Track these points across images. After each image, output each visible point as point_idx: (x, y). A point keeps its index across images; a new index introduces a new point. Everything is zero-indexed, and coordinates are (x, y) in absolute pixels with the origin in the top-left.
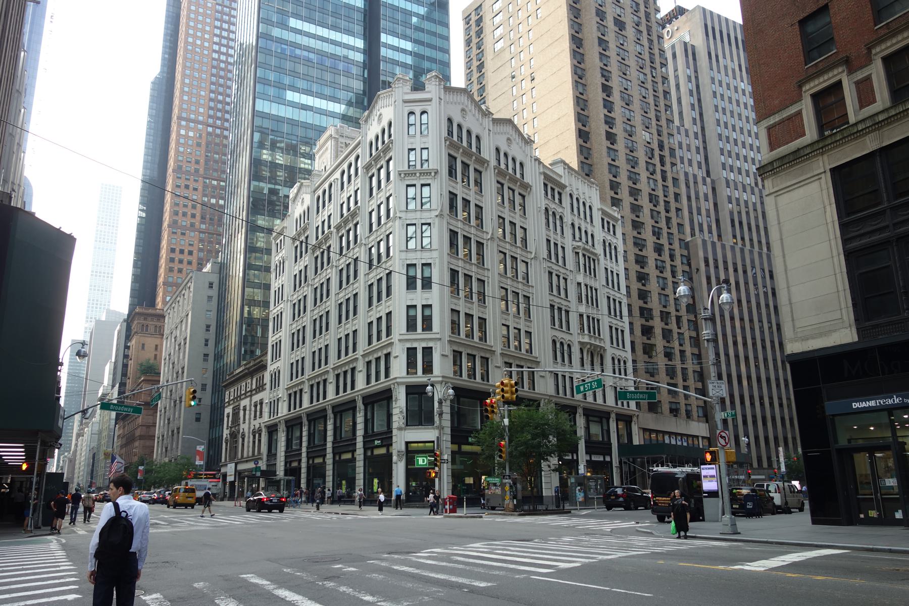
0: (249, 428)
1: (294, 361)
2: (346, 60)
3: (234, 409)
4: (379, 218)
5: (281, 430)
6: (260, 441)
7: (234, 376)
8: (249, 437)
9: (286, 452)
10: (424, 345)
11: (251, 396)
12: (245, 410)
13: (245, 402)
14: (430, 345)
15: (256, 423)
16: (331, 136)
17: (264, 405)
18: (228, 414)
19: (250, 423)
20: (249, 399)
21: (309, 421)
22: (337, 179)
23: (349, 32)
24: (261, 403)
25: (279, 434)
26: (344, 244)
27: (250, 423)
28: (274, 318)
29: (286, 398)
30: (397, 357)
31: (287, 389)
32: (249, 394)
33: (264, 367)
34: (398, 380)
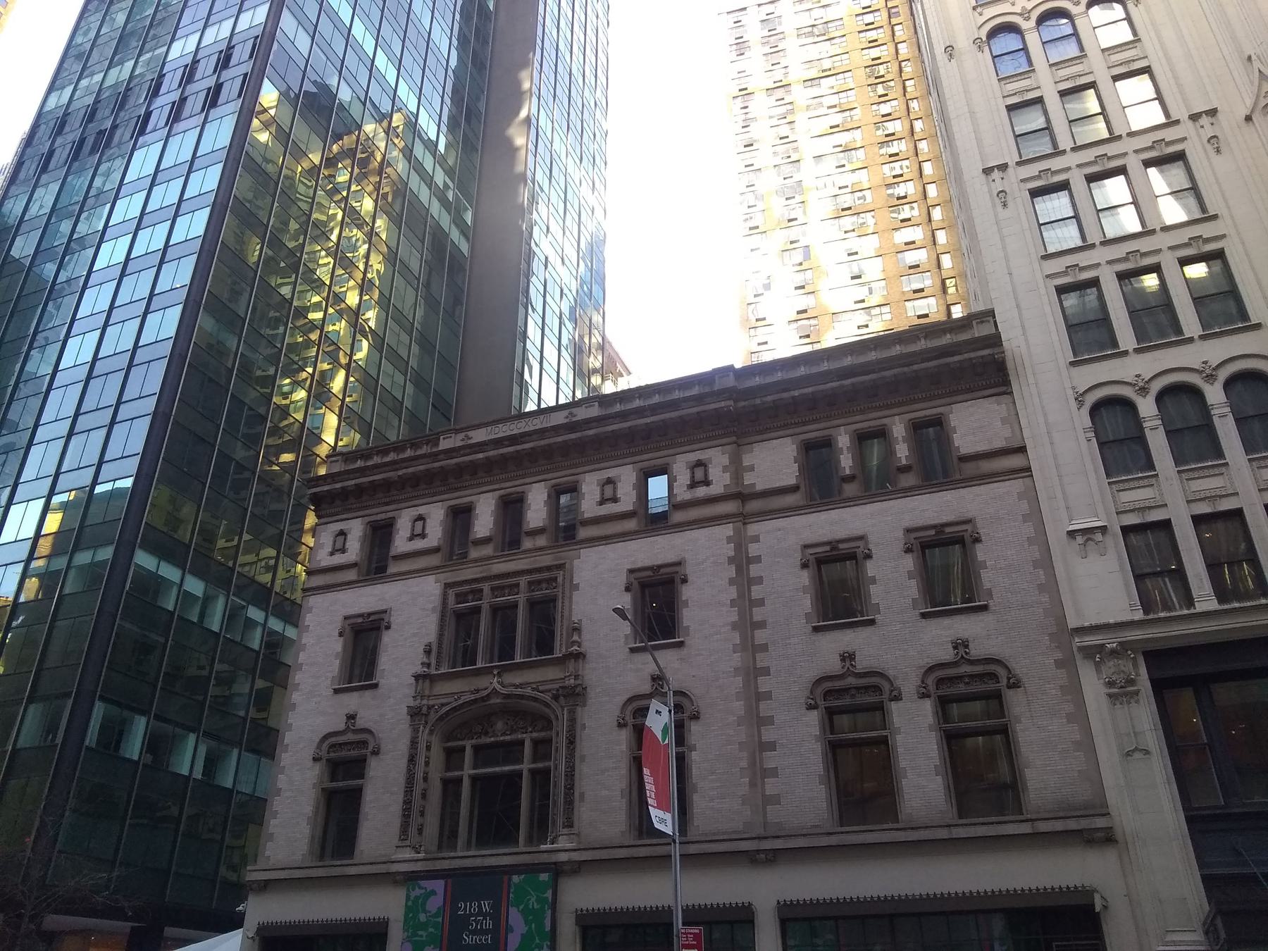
7: (435, 456)
11: (744, 518)
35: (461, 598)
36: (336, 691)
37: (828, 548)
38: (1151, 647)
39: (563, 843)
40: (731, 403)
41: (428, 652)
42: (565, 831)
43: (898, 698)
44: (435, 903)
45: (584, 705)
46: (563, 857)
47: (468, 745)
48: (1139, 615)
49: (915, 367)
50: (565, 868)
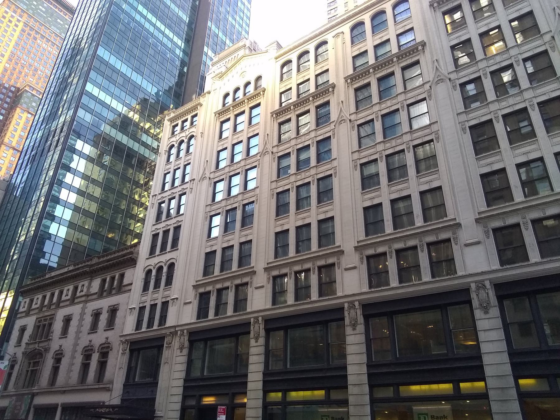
0: (76, 345)
3: (39, 320)
6: (102, 365)
8: (73, 357)
9: (186, 381)
11: (86, 302)
12: (67, 320)
13: (75, 310)
15: (98, 339)
16: (245, 46)
17: (119, 314)
18: (23, 330)
20: (81, 305)
22: (343, 33)
24: (113, 311)
25: (166, 353)
27: (77, 338)
31: (195, 287)
33: (132, 262)
35: (39, 322)
36: (60, 338)
37: (96, 311)
38: (132, 341)
39: (36, 388)
40: (88, 269)
41: (30, 337)
42: (37, 385)
43: (94, 353)
44: (13, 402)
45: (48, 353)
46: (35, 391)
47: (32, 361)
48: (134, 332)
49: (119, 259)
50: (35, 394)
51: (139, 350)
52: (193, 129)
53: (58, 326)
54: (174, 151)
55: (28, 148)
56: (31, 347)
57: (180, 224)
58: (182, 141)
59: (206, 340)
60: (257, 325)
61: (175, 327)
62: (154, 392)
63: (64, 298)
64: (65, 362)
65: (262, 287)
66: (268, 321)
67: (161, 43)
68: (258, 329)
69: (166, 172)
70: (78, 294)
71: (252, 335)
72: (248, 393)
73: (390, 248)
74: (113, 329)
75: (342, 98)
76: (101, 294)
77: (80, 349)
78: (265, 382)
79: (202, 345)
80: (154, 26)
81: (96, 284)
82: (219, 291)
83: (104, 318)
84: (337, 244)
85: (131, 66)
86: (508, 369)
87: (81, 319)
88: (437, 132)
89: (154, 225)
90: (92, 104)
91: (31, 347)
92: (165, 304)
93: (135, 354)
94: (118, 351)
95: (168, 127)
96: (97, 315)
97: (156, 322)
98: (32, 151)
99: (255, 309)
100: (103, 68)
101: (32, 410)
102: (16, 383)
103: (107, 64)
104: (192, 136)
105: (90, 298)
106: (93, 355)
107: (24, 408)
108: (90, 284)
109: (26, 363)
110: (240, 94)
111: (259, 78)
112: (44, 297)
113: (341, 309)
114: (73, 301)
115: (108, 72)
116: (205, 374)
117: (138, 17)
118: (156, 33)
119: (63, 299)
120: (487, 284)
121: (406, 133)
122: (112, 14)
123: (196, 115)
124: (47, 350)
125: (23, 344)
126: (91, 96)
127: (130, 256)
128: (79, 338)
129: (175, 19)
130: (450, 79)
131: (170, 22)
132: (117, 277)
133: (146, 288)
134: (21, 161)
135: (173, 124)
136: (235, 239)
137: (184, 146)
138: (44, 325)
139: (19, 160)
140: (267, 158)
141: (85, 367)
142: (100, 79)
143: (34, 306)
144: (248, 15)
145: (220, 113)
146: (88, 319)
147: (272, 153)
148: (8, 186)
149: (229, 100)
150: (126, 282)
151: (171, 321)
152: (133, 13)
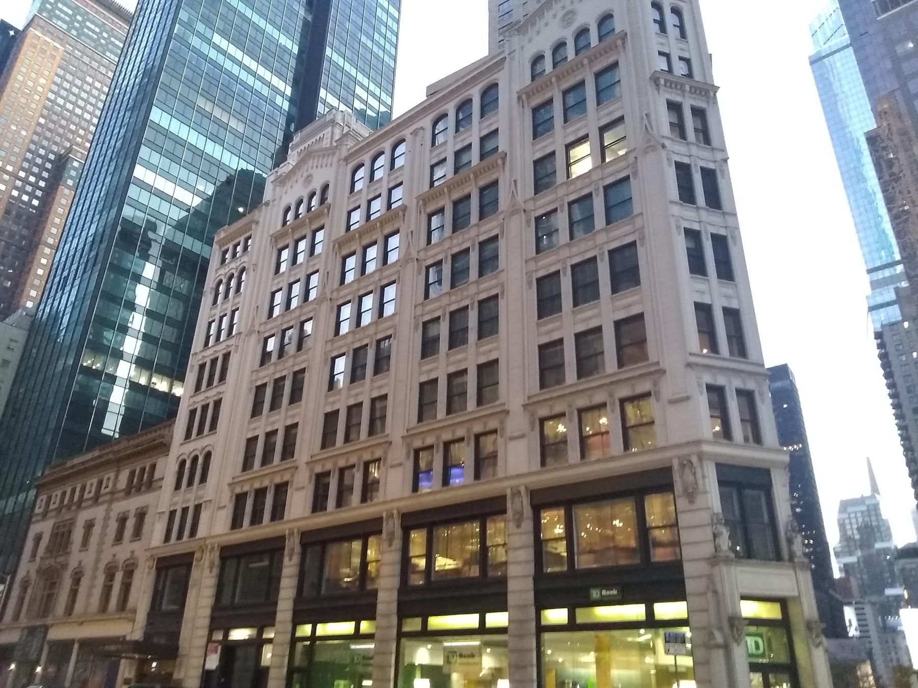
0: (98, 560)
1: (341, 404)
2: (272, 104)
3: (56, 527)
4: (219, 331)
5: (206, 563)
6: (126, 587)
10: (737, 383)
11: (111, 502)
13: (98, 513)
14: (750, 385)
15: (123, 552)
17: (147, 519)
18: (38, 538)
19: (99, 552)
20: (105, 507)
21: (304, 546)
22: (422, 128)
23: (280, 75)
24: (141, 516)
25: (195, 574)
26: (213, 331)
27: (99, 552)
28: (202, 367)
29: (227, 500)
30: (688, 398)
32: (107, 498)
33: (163, 447)
34: (706, 448)
48: (162, 545)
51: (167, 568)
52: (245, 259)
53: (78, 534)
54: (222, 288)
55: (58, 266)
56: (47, 562)
57: (221, 396)
58: (232, 276)
59: (239, 557)
60: (292, 539)
61: (204, 539)
62: (179, 623)
63: (86, 496)
64: (85, 582)
65: (303, 488)
66: (304, 535)
67: (252, 89)
68: (293, 545)
69: (210, 320)
70: (103, 491)
71: (286, 552)
72: (277, 624)
73: (611, 395)
74: (140, 540)
75: (413, 228)
76: (129, 491)
77: (102, 565)
78: (400, 604)
79: (235, 561)
80: (240, 64)
81: (124, 476)
82: (342, 471)
83: (130, 524)
84: (386, 433)
85: (205, 133)
86: (531, 596)
87: (105, 526)
88: (502, 286)
89: (192, 397)
90: (144, 197)
91: (47, 562)
92: (198, 508)
93: (163, 574)
94: (144, 569)
95: (217, 253)
96: (123, 520)
97: (187, 532)
98: (63, 270)
99: (292, 517)
100: (160, 139)
101: (46, 649)
102: (28, 611)
103: (166, 133)
104: (243, 270)
105: (116, 496)
106: (117, 574)
107: (35, 644)
108: (117, 477)
109: (42, 583)
110: (302, 209)
111: (325, 188)
112: (64, 494)
113: (503, 498)
114: (96, 500)
115: (168, 145)
116: (236, 600)
117: (213, 54)
118: (244, 75)
119: (85, 498)
120: (522, 489)
121: (473, 283)
122: (173, 54)
123: (250, 237)
124: (64, 567)
125: (38, 559)
126: (144, 186)
127: (162, 440)
128: (101, 552)
129: (273, 48)
130: (525, 211)
131: (266, 55)
132: (147, 469)
133: (178, 486)
134: (49, 286)
135: (224, 249)
136: (365, 392)
137: (233, 283)
138: (63, 534)
139: (47, 282)
140: (325, 307)
141: (108, 589)
142: (155, 158)
143: (52, 507)
144: (395, 29)
145: (276, 238)
146: (113, 526)
147: (331, 299)
148: (33, 323)
149: (290, 216)
150: (157, 475)
151: (202, 532)
152: (205, 49)
